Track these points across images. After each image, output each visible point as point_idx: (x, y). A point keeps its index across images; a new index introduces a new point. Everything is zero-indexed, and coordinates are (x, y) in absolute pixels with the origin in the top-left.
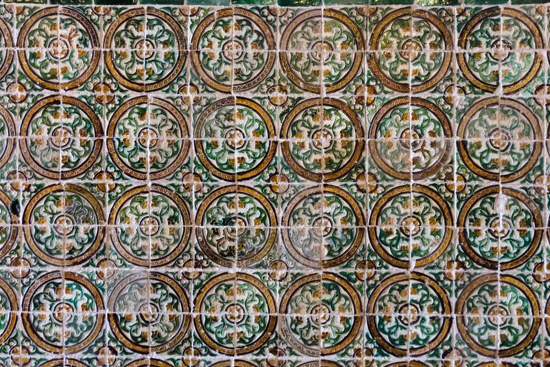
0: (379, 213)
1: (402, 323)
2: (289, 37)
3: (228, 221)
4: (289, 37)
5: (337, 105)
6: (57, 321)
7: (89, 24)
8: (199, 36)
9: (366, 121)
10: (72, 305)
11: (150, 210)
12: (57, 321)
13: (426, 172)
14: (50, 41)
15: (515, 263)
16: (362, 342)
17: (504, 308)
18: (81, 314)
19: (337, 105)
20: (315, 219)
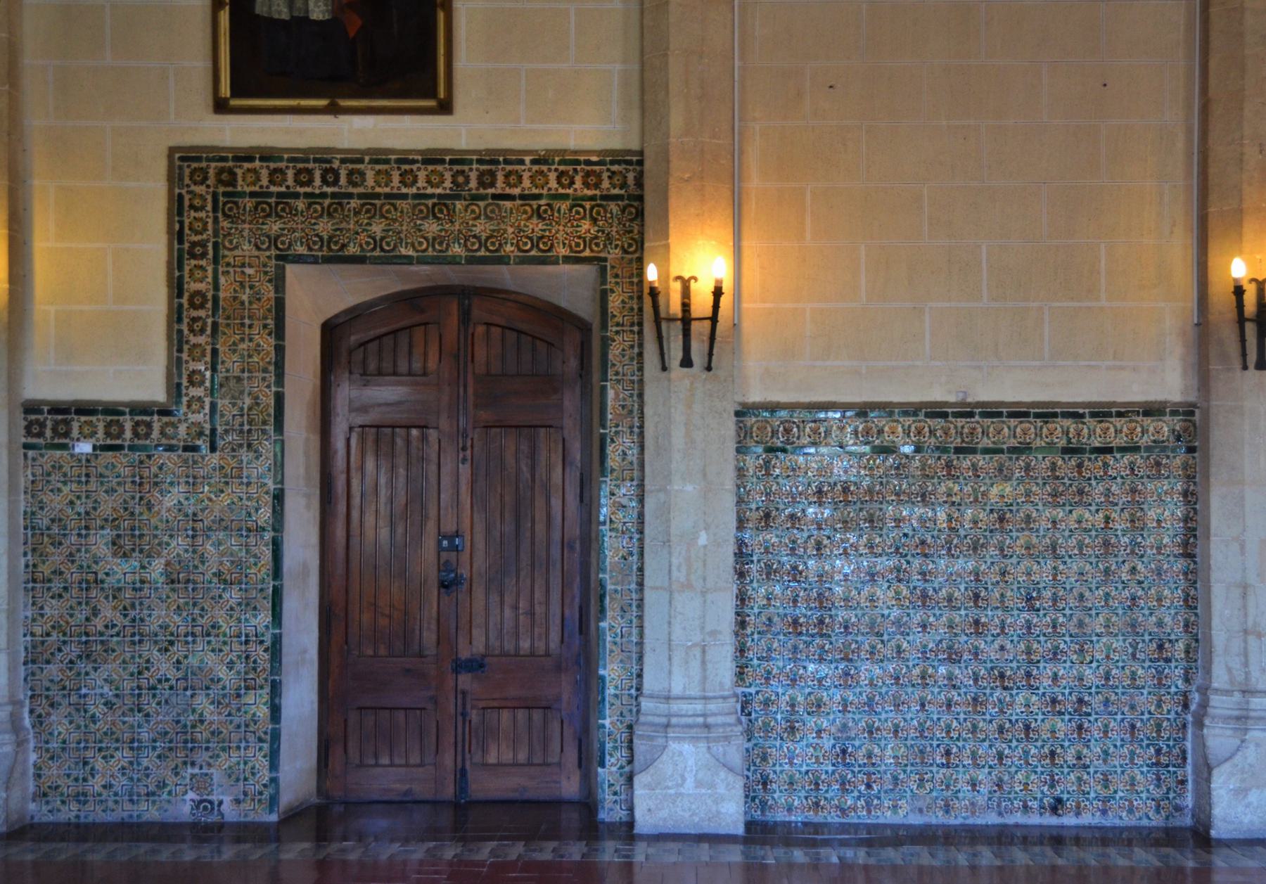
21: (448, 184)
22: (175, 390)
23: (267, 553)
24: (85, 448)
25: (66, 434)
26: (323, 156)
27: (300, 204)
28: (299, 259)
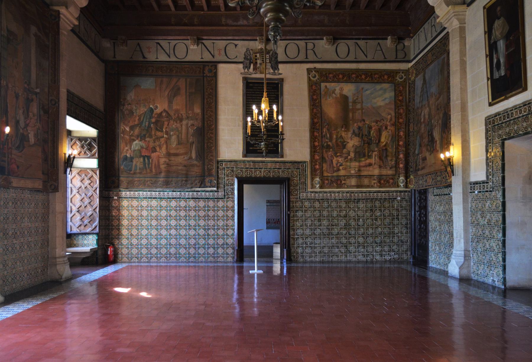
0: (349, 221)
1: (351, 232)
2: (340, 203)
3: (334, 222)
4: (340, 203)
5: (344, 210)
6: (317, 233)
7: (320, 202)
8: (331, 203)
9: (347, 212)
10: (318, 231)
11: (326, 221)
12: (317, 233)
13: (353, 217)
14: (316, 204)
15: (362, 226)
16: (348, 234)
17: (361, 230)
18: (319, 232)
19: (344, 210)
20: (343, 222)
21: (527, 111)
22: (487, 177)
23: (501, 218)
24: (476, 192)
25: (474, 189)
26: (506, 111)
27: (504, 125)
28: (505, 139)
